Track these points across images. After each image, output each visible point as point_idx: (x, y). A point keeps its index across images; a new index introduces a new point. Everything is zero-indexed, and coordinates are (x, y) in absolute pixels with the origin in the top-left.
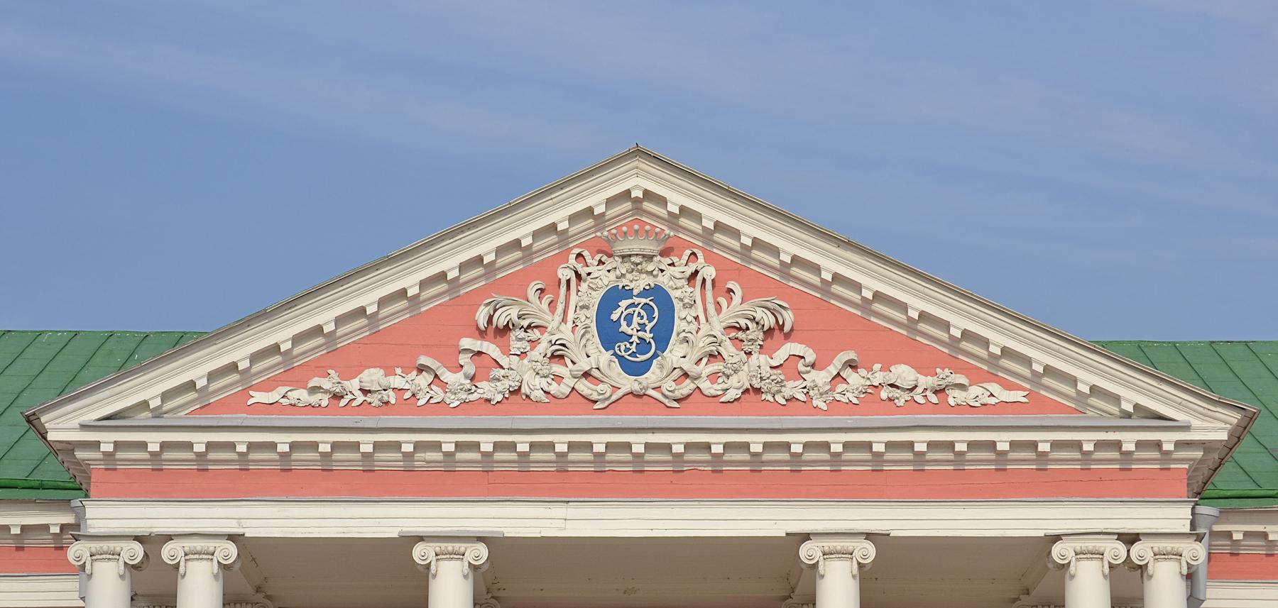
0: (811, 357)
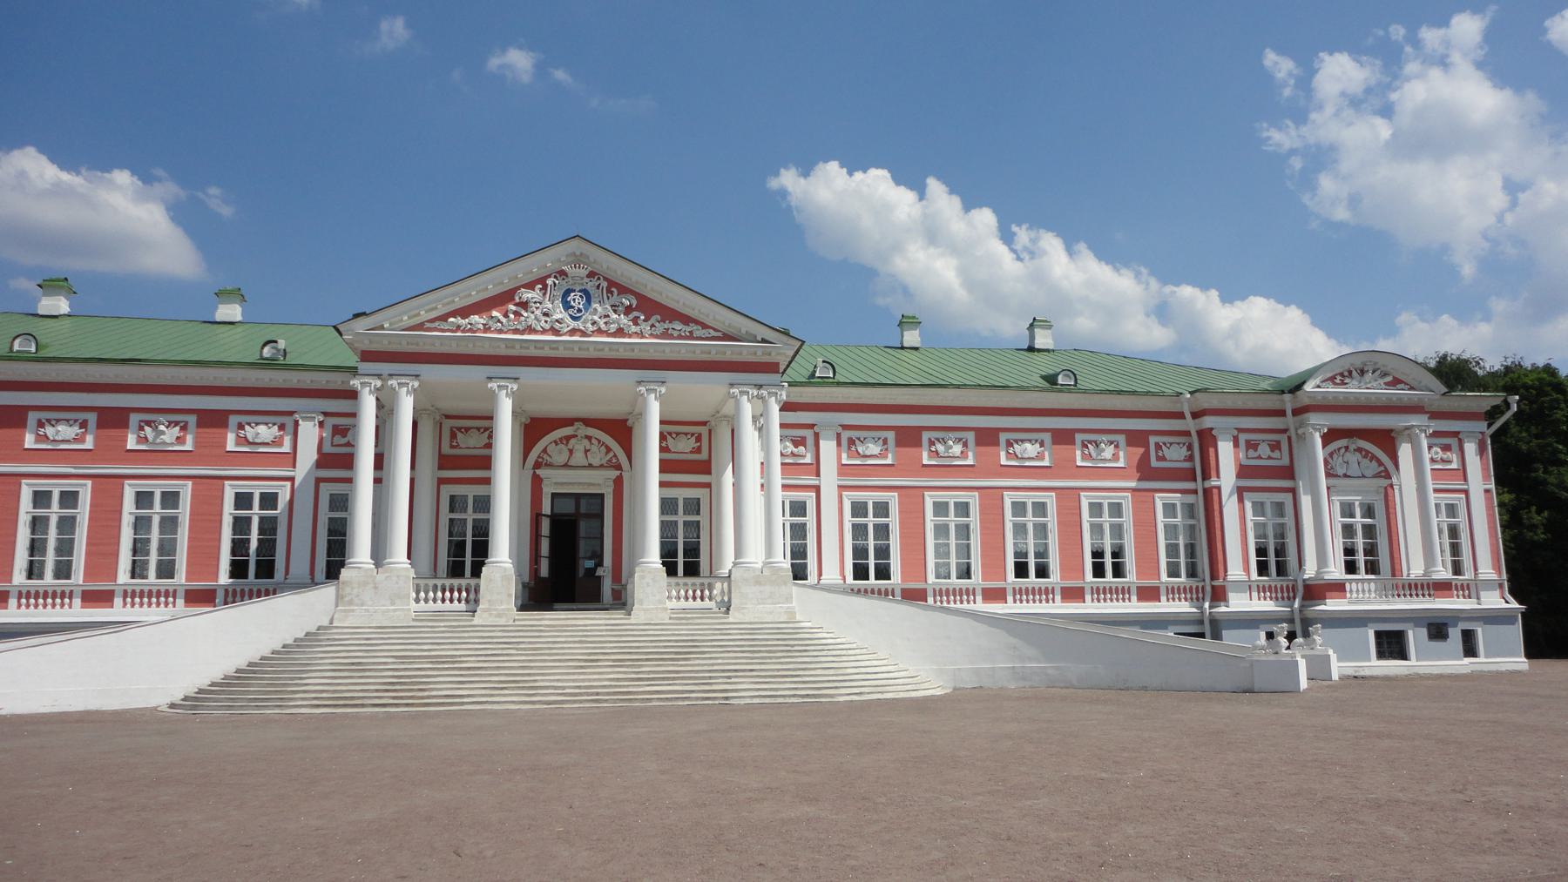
0: (642, 317)
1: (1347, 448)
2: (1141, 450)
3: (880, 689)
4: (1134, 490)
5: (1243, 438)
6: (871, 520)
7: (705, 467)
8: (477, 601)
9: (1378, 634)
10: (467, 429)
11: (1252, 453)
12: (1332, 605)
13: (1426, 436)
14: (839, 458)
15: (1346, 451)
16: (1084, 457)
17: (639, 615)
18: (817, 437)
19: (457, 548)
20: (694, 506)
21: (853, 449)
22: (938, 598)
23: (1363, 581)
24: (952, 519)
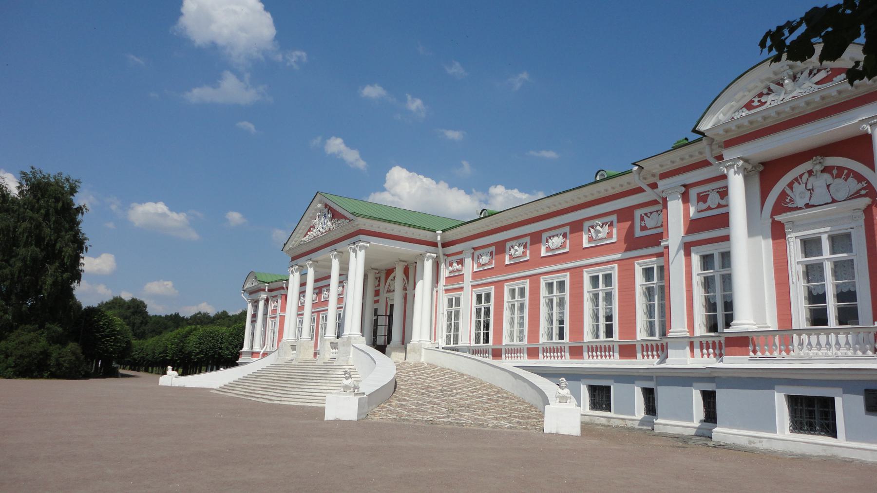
9: (794, 401)
15: (810, 175)
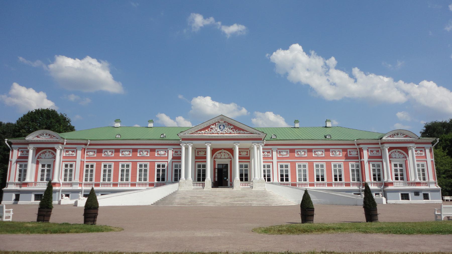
1: (395, 151)
2: (346, 153)
3: (281, 204)
4: (344, 161)
5: (369, 150)
6: (284, 169)
7: (249, 158)
8: (204, 186)
9: (402, 194)
10: (201, 151)
11: (372, 153)
12: (390, 187)
13: (414, 149)
14: (277, 155)
15: (395, 152)
16: (332, 154)
17: (235, 189)
18: (272, 151)
19: (199, 175)
20: (246, 166)
21: (280, 154)
22: (299, 185)
23: (399, 182)
24: (302, 168)
